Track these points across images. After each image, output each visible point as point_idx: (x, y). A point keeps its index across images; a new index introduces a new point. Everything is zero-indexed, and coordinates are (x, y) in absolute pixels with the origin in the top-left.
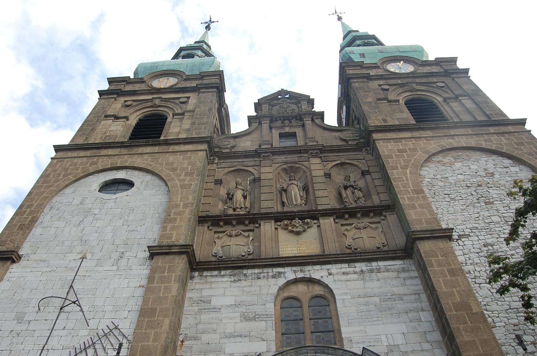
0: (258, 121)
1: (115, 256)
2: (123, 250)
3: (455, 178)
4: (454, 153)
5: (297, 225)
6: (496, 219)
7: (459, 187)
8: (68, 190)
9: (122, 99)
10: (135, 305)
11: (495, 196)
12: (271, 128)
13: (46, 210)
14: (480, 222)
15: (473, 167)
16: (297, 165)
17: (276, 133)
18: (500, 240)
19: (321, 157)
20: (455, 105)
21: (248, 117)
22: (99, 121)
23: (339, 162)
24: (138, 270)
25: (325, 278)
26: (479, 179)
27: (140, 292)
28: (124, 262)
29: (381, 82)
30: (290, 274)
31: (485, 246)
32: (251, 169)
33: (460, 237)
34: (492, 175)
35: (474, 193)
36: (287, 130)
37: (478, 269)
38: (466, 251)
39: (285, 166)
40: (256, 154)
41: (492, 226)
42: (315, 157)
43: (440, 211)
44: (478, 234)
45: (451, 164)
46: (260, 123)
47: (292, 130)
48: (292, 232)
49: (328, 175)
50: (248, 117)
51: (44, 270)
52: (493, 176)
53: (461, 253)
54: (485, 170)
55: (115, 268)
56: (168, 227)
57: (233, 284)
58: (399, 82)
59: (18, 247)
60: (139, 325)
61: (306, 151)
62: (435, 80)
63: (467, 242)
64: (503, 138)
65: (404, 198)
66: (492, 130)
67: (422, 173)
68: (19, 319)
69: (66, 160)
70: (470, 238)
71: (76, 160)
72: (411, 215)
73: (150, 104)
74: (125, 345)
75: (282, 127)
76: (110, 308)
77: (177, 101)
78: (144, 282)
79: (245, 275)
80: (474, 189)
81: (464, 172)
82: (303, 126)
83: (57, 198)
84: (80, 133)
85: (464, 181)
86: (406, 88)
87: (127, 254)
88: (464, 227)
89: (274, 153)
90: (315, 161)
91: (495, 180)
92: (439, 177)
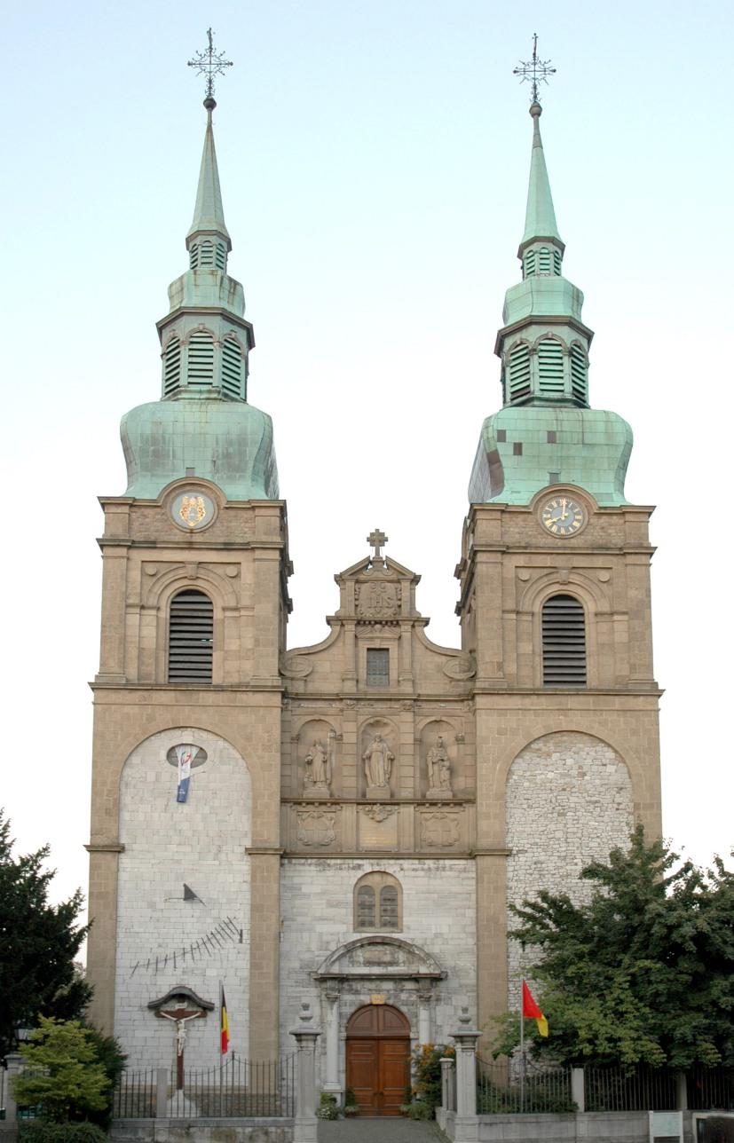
0: (340, 623)
1: (214, 849)
2: (217, 843)
3: (543, 776)
4: (558, 737)
6: (558, 835)
7: (542, 790)
8: (136, 759)
9: (138, 556)
10: (246, 898)
11: (572, 805)
13: (123, 789)
14: (543, 837)
15: (569, 762)
16: (386, 721)
17: (364, 645)
18: (552, 858)
20: (604, 627)
21: (327, 617)
22: (123, 621)
23: (433, 719)
24: (243, 866)
26: (567, 780)
27: (246, 887)
28: (223, 856)
29: (521, 560)
31: (535, 863)
33: (519, 852)
34: (584, 774)
35: (554, 800)
36: (377, 644)
37: (519, 886)
38: (517, 868)
41: (551, 843)
42: (408, 710)
43: (512, 820)
44: (535, 850)
45: (549, 755)
50: (327, 617)
51: (153, 861)
52: (583, 777)
53: (512, 869)
54: (580, 767)
55: (217, 862)
56: (258, 823)
57: (319, 874)
58: (548, 560)
59: (118, 837)
60: (252, 918)
62: (599, 561)
63: (522, 858)
64: (622, 719)
65: (482, 804)
66: (617, 702)
67: (515, 767)
68: (152, 906)
69: (113, 707)
70: (526, 854)
71: (126, 709)
72: (484, 825)
73: (181, 573)
74: (244, 932)
75: (372, 639)
76: (224, 901)
77: (220, 570)
78: (248, 878)
79: (329, 865)
80: (555, 794)
81: (557, 769)
83: (127, 771)
84: (108, 647)
85: (551, 782)
86: (554, 578)
87: (224, 848)
88: (526, 841)
90: (408, 717)
91: (584, 782)
92: (528, 773)
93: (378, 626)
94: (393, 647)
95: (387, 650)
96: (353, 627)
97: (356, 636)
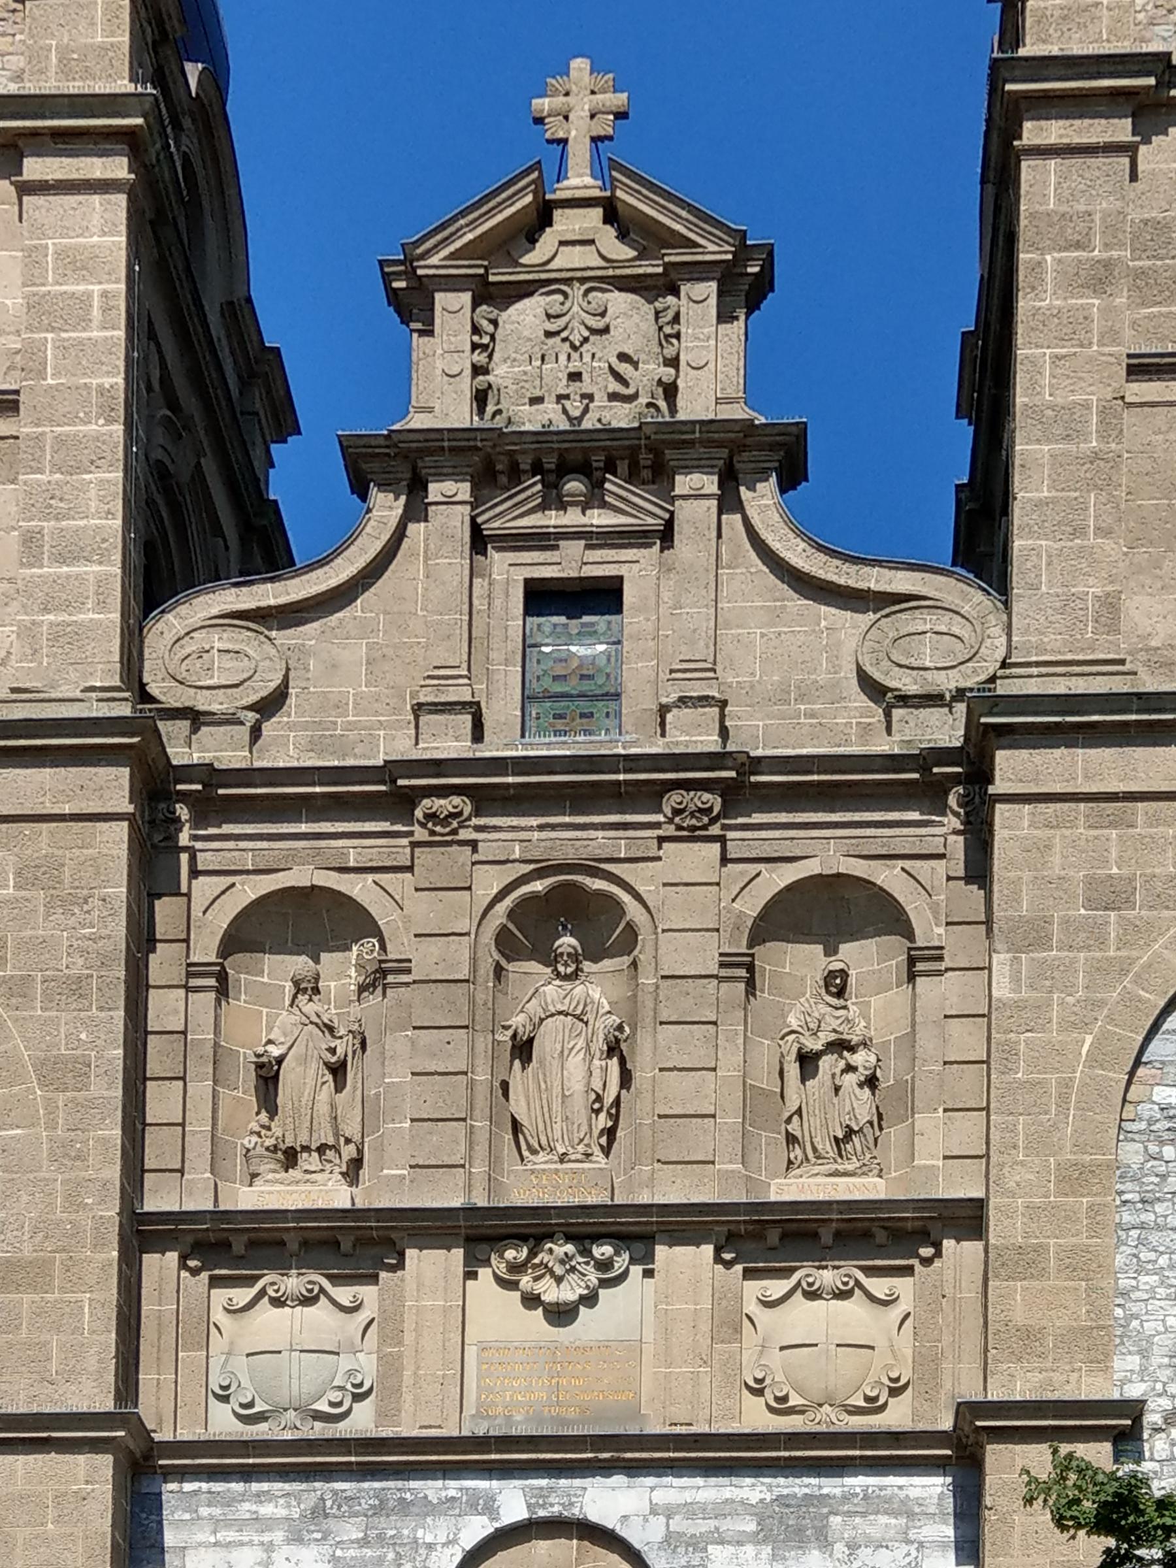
5: (559, 1270)
12: (479, 541)
17: (509, 571)
19: (722, 840)
25: (636, 1521)
30: (513, 1501)
32: (358, 888)
39: (538, 886)
40: (391, 794)
42: (693, 836)
46: (416, 488)
47: (599, 564)
48: (531, 1301)
49: (743, 970)
61: (651, 795)
75: (543, 540)
82: (666, 535)
89: (488, 800)
93: (574, 486)
94: (636, 569)
95: (620, 579)
96: (463, 490)
97: (476, 529)
